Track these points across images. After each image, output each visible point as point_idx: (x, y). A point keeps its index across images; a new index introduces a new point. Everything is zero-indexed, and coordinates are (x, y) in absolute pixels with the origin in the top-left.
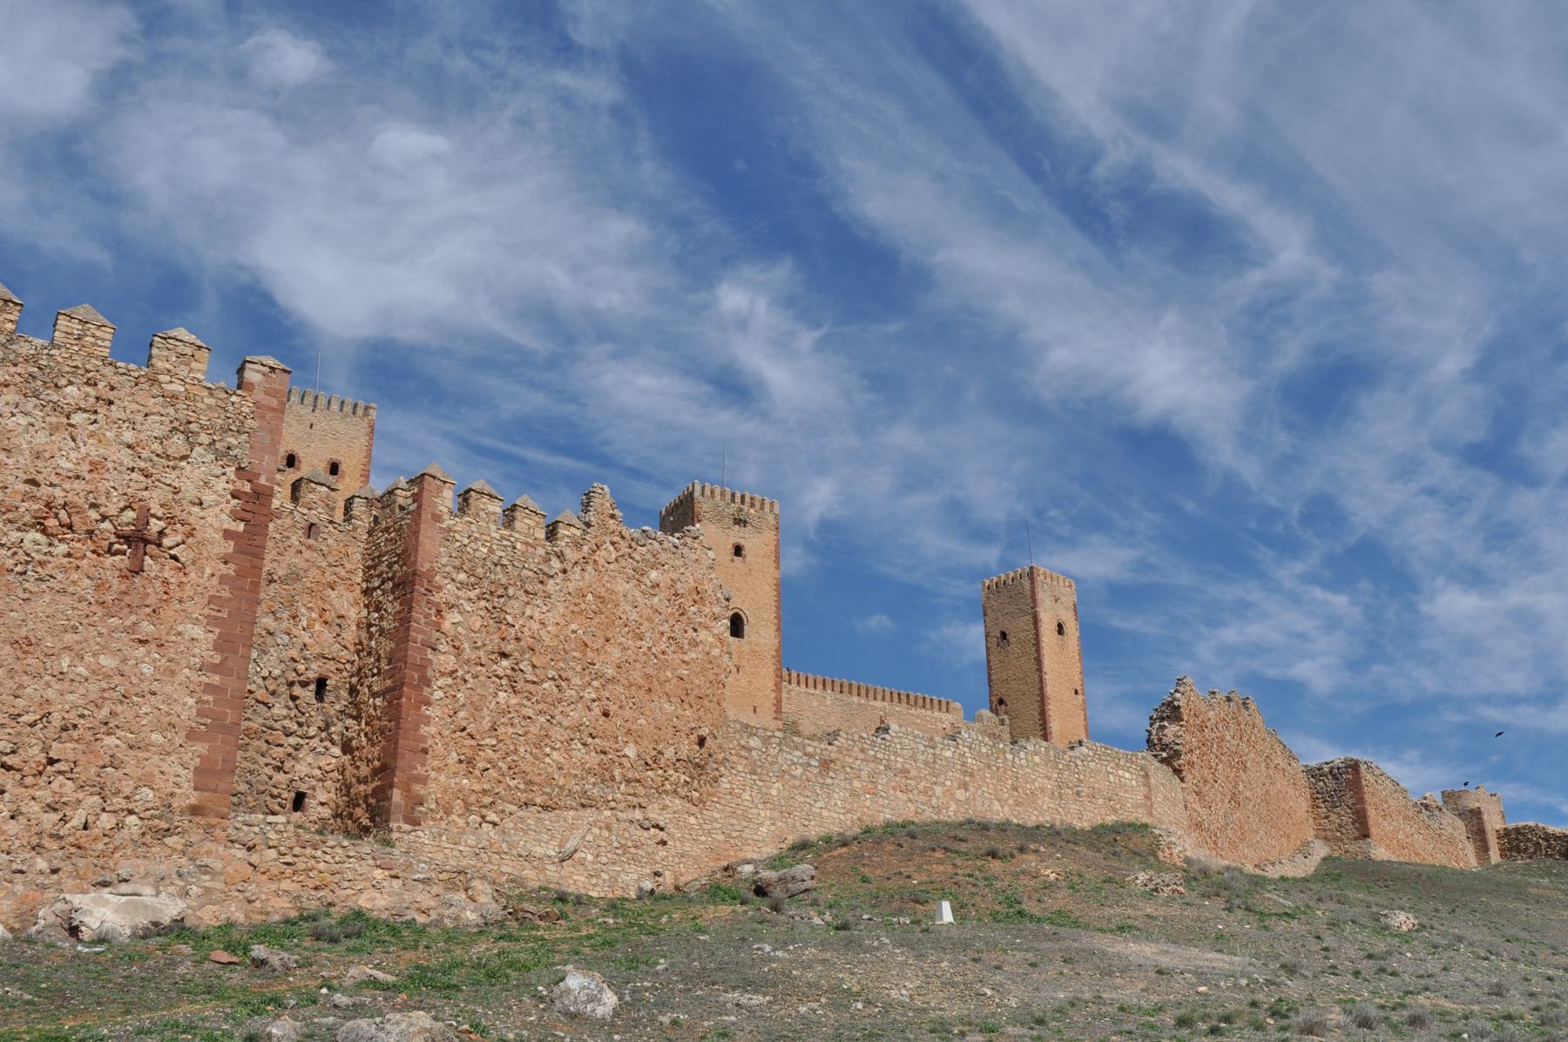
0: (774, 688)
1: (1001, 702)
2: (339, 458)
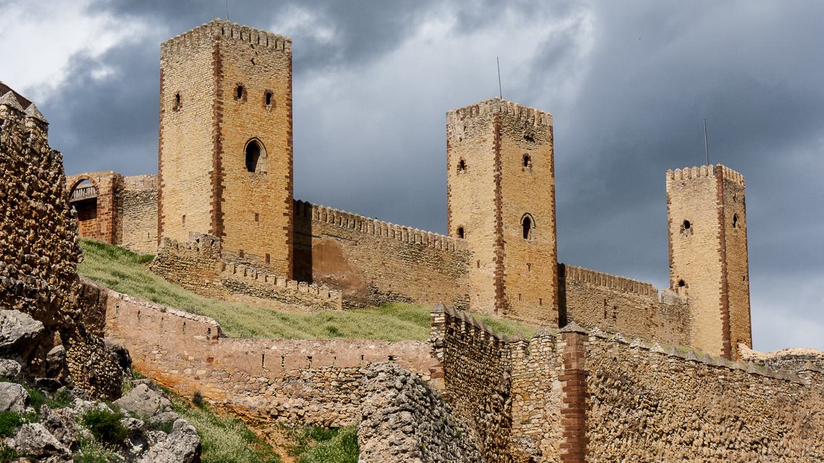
0: (552, 283)
1: (682, 283)
2: (272, 89)
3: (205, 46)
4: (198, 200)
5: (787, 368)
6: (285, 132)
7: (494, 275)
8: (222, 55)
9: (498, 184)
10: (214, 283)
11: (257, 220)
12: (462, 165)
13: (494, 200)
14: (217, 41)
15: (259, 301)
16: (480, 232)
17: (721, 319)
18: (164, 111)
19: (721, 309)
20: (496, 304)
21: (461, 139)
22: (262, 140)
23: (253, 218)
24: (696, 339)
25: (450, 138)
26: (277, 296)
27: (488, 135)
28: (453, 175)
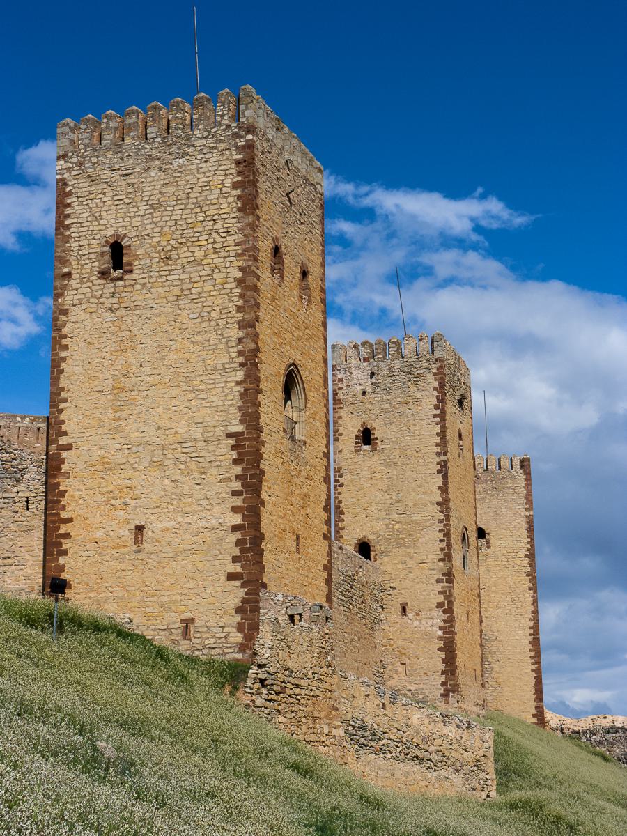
3: (212, 142)
4: (191, 496)
5: (612, 744)
6: (321, 359)
7: (440, 633)
8: (257, 169)
9: (445, 477)
10: (335, 732)
11: (298, 552)
12: (366, 437)
13: (438, 504)
14: (250, 137)
15: (401, 768)
16: (409, 554)
17: (532, 671)
18: (69, 275)
19: (531, 657)
20: (443, 684)
21: (364, 393)
22: (299, 367)
23: (295, 545)
24: (494, 696)
25: (342, 388)
26: (419, 754)
27: (423, 393)
28: (345, 451)
